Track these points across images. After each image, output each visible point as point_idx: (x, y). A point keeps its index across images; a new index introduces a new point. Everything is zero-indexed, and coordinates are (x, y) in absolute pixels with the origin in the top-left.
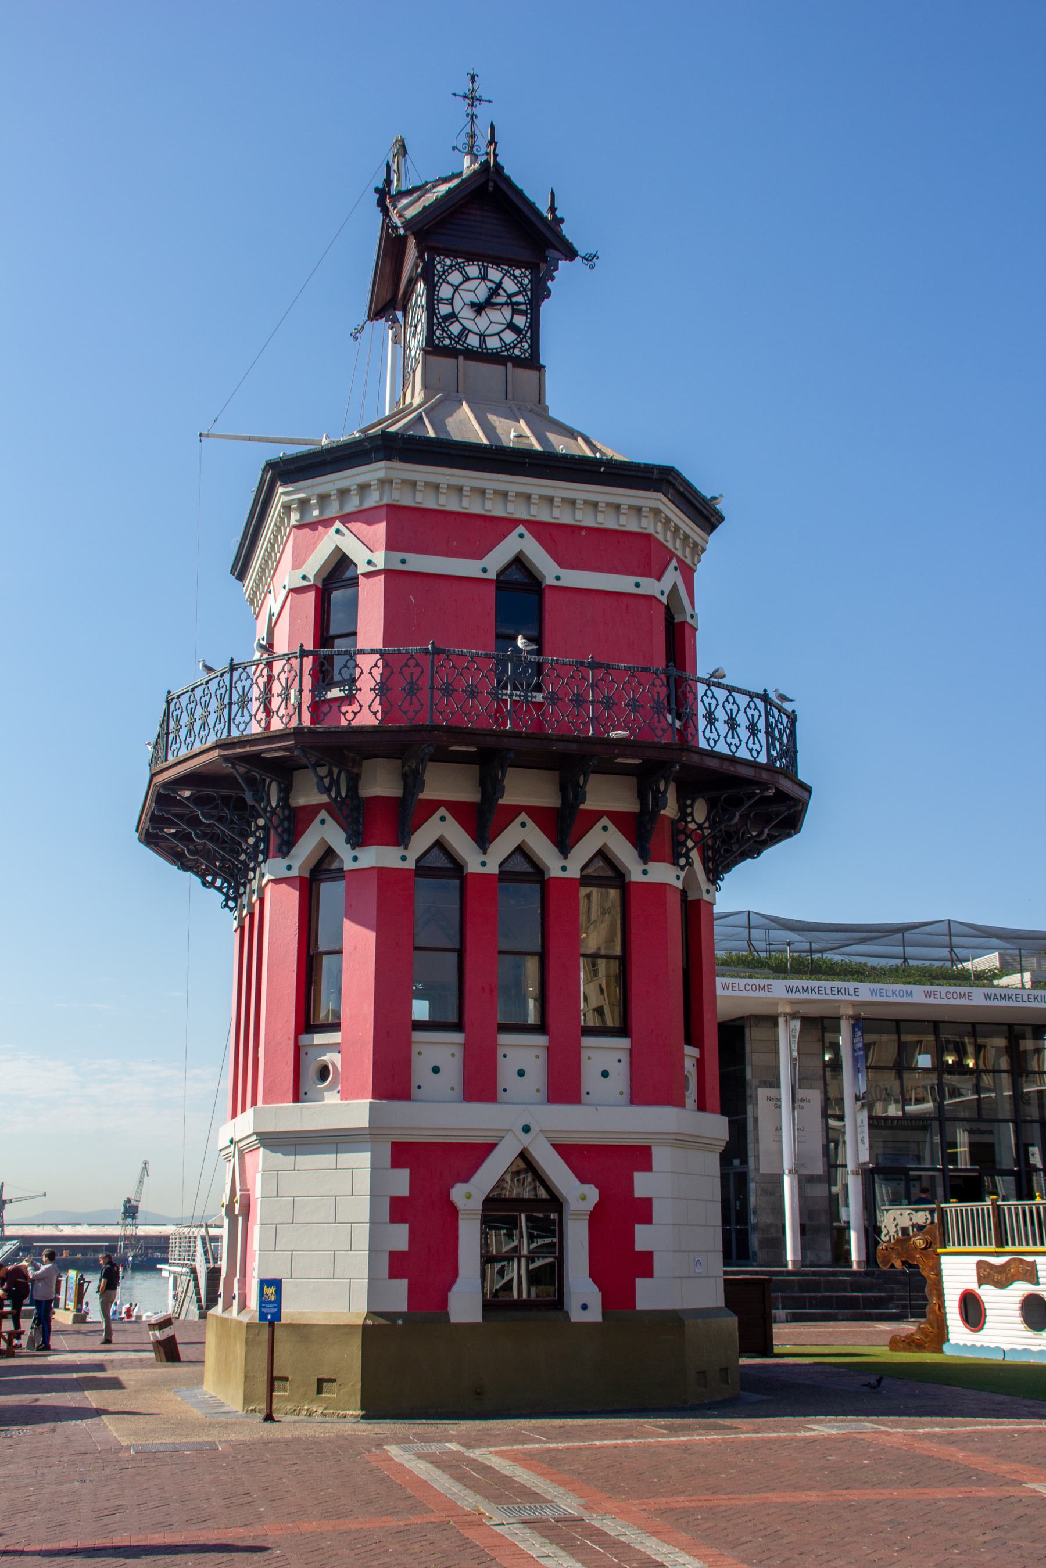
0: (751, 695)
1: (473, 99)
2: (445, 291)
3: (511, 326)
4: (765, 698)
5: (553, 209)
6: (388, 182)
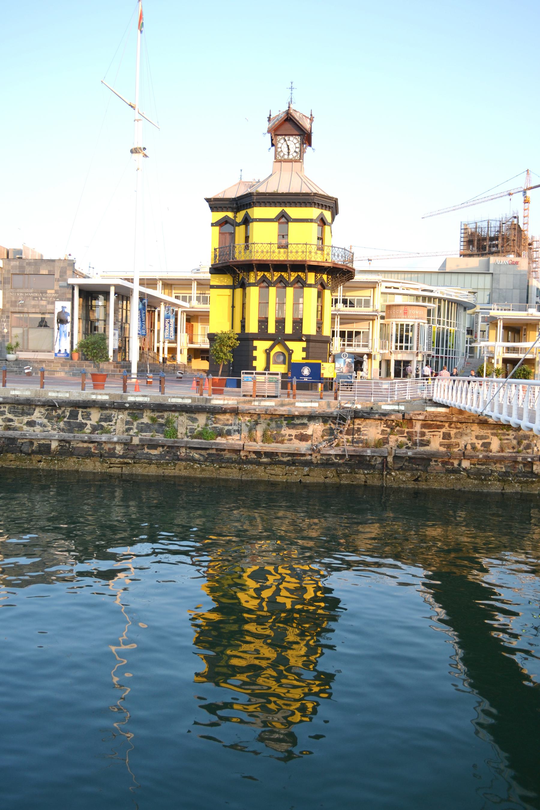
0: (328, 246)
1: (292, 88)
2: (279, 145)
3: (295, 152)
4: (332, 247)
5: (311, 115)
6: (270, 115)
